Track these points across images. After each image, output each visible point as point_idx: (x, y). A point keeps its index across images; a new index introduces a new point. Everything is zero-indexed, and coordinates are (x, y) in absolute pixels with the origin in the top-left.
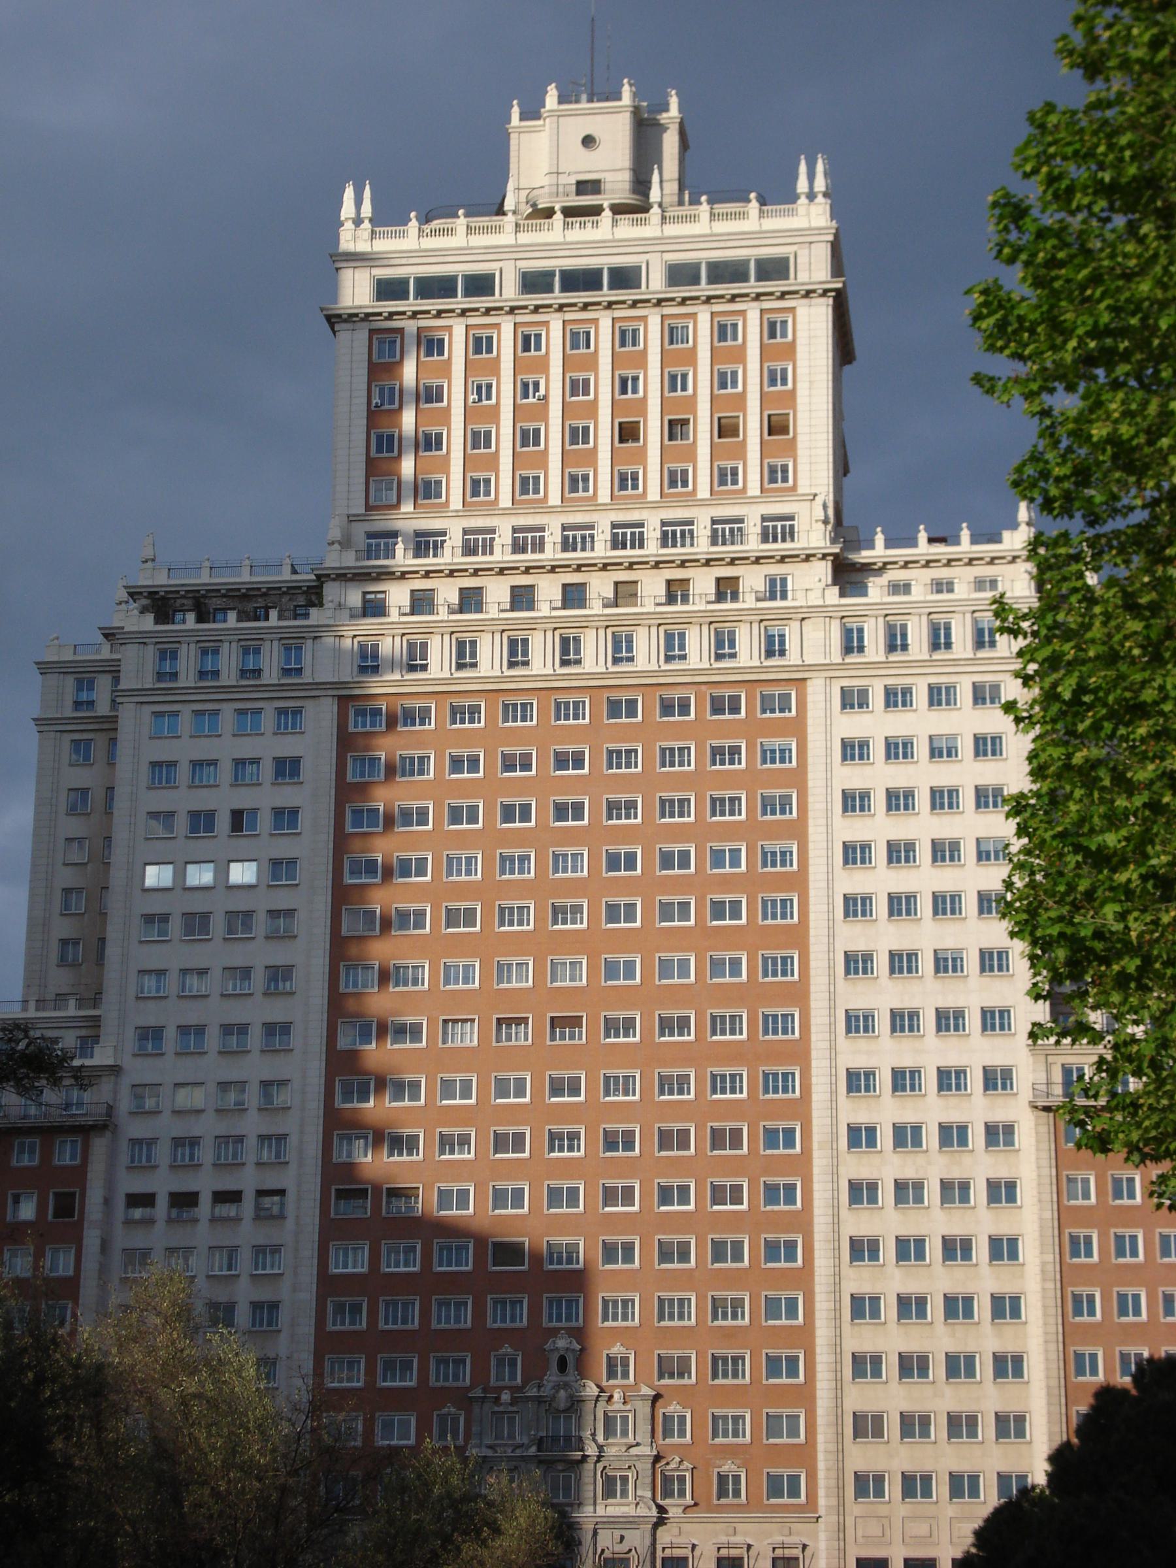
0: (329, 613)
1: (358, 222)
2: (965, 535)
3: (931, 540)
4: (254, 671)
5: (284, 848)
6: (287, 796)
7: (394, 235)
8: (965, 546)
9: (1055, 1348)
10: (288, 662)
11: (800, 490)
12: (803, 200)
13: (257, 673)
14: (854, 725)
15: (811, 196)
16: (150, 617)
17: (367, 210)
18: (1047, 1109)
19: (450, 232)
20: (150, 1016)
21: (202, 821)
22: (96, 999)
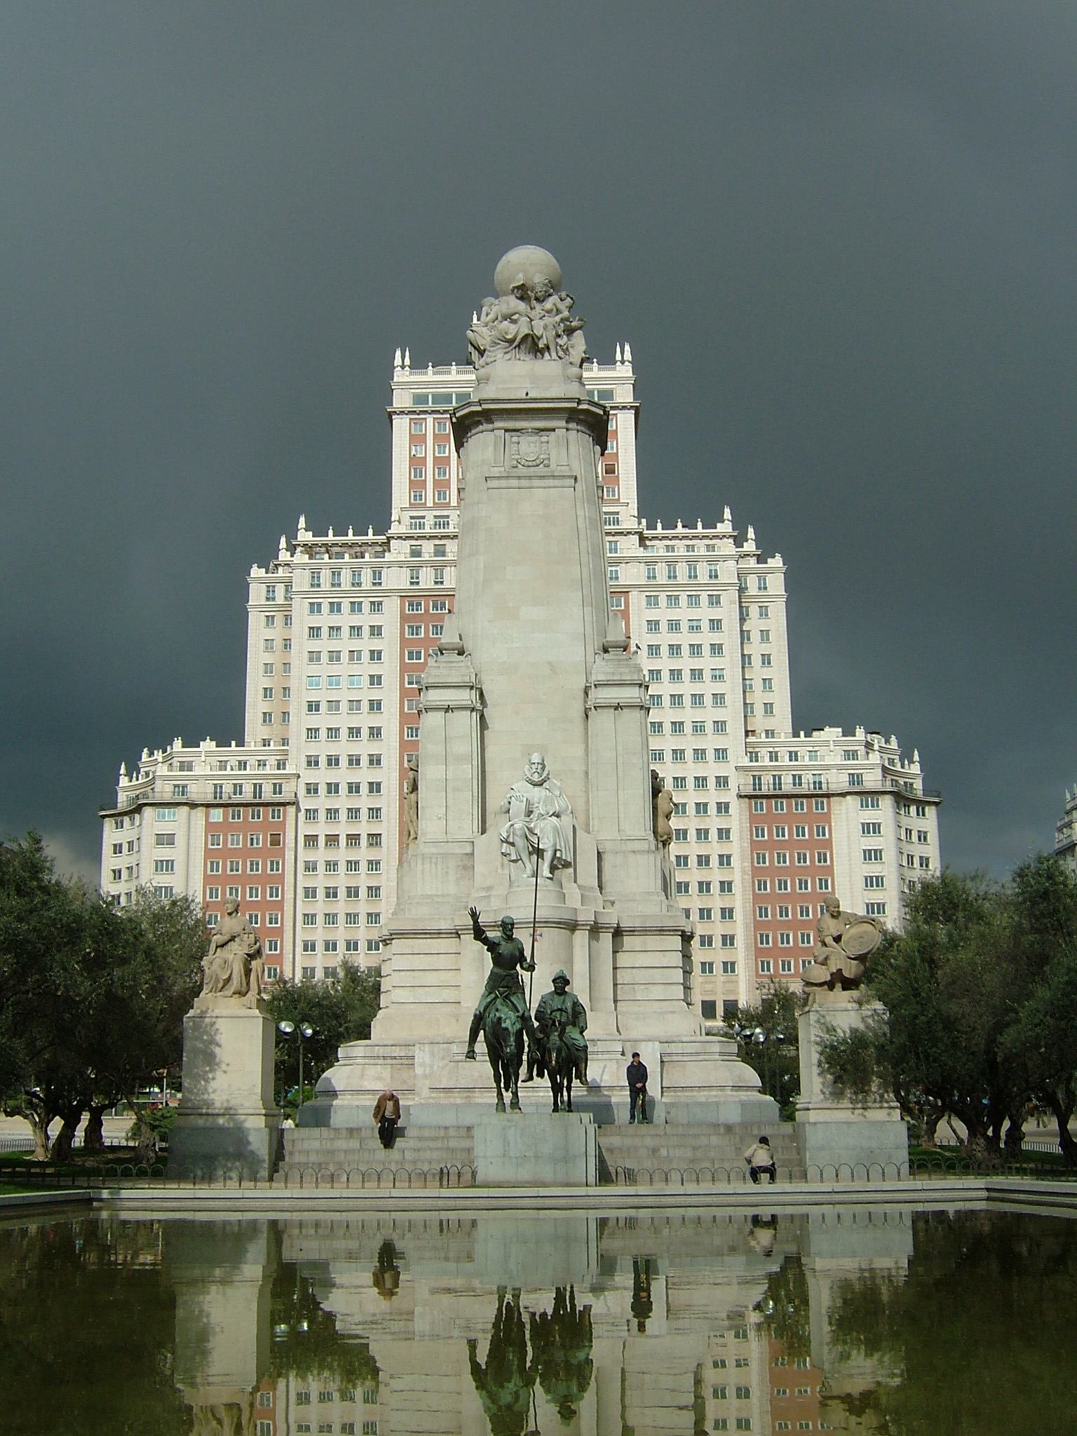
0: (395, 555)
1: (403, 367)
2: (700, 525)
3: (683, 527)
4: (358, 584)
5: (375, 669)
6: (376, 644)
7: (420, 374)
8: (680, 529)
9: (749, 906)
10: (375, 579)
11: (621, 501)
12: (619, 363)
13: (359, 584)
14: (653, 614)
15: (623, 362)
16: (307, 556)
17: (407, 361)
18: (746, 796)
19: (449, 373)
20: (312, 749)
21: (335, 656)
22: (285, 742)
